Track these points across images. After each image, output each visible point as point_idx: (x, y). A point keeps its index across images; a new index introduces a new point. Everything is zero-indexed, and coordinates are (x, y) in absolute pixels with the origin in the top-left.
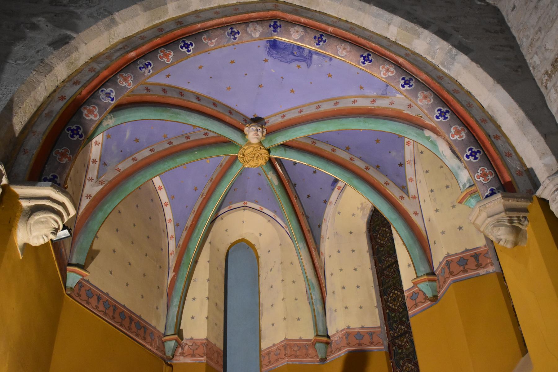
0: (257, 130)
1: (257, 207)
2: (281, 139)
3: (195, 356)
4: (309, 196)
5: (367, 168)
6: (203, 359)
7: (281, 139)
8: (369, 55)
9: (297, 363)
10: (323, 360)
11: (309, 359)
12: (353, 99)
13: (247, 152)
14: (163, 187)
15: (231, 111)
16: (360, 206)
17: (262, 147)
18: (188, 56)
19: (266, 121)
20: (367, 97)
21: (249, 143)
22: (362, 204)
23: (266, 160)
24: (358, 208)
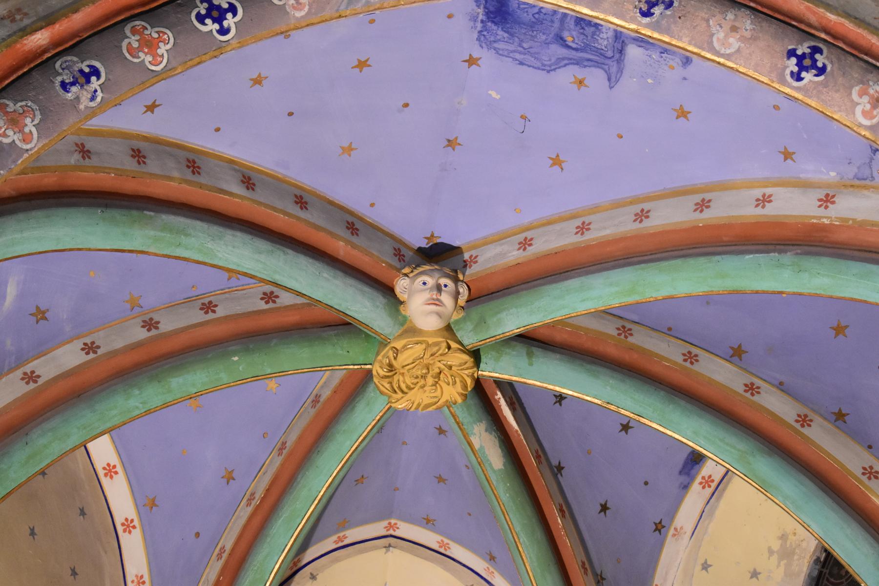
0: (439, 288)
1: (431, 538)
2: (515, 318)
4: (604, 508)
5: (804, 420)
7: (515, 318)
8: (816, 50)
12: (758, 193)
13: (405, 358)
14: (119, 468)
15: (354, 224)
16: (776, 545)
17: (454, 345)
18: (221, 48)
19: (466, 256)
20: (805, 185)
21: (412, 331)
22: (783, 537)
23: (465, 387)
24: (771, 552)
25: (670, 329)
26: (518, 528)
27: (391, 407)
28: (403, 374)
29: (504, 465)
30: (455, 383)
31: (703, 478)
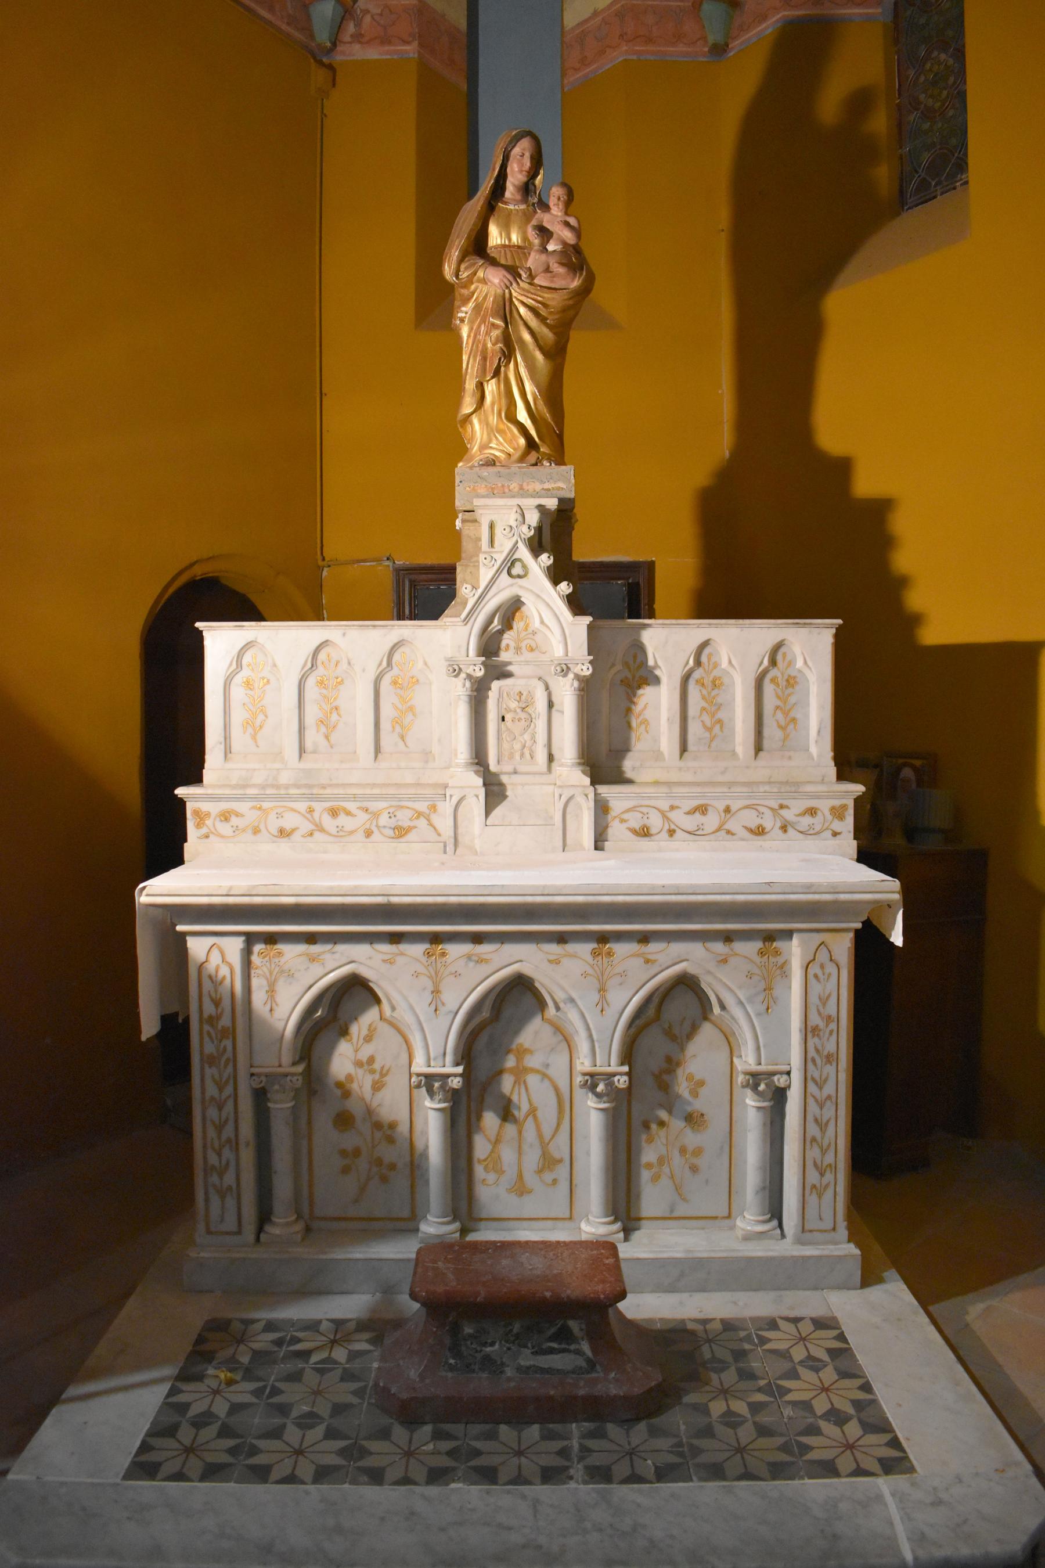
3: (389, 43)
6: (411, 50)
9: (652, 58)
10: (719, 50)
11: (681, 48)
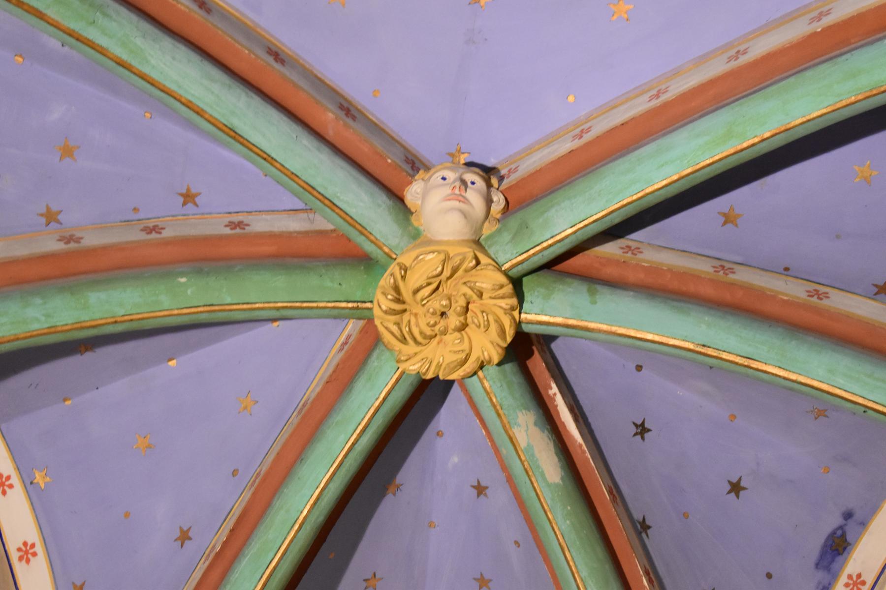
7: (566, 219)
13: (416, 279)
14: (39, 549)
15: (348, 109)
23: (502, 332)
25: (787, 269)
26: (584, 574)
27: (403, 373)
28: (416, 315)
29: (562, 479)
30: (487, 327)
31: (850, 577)
